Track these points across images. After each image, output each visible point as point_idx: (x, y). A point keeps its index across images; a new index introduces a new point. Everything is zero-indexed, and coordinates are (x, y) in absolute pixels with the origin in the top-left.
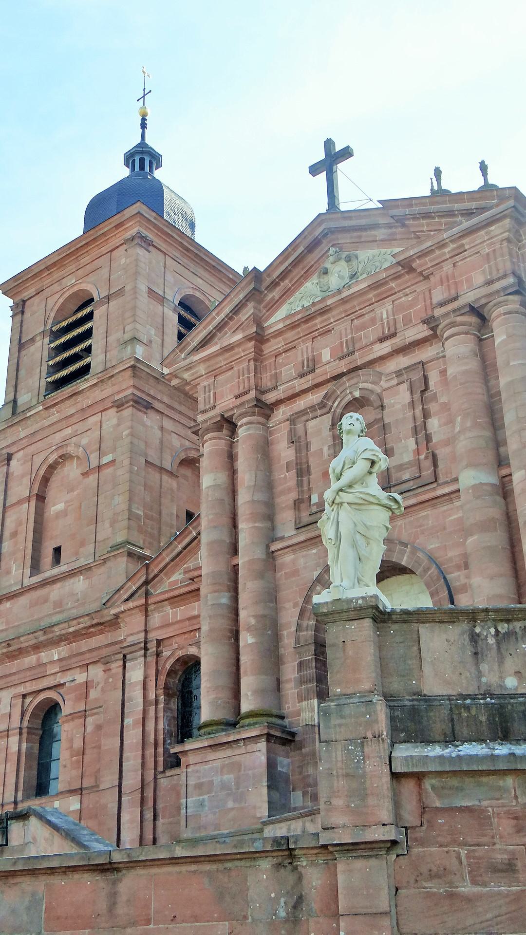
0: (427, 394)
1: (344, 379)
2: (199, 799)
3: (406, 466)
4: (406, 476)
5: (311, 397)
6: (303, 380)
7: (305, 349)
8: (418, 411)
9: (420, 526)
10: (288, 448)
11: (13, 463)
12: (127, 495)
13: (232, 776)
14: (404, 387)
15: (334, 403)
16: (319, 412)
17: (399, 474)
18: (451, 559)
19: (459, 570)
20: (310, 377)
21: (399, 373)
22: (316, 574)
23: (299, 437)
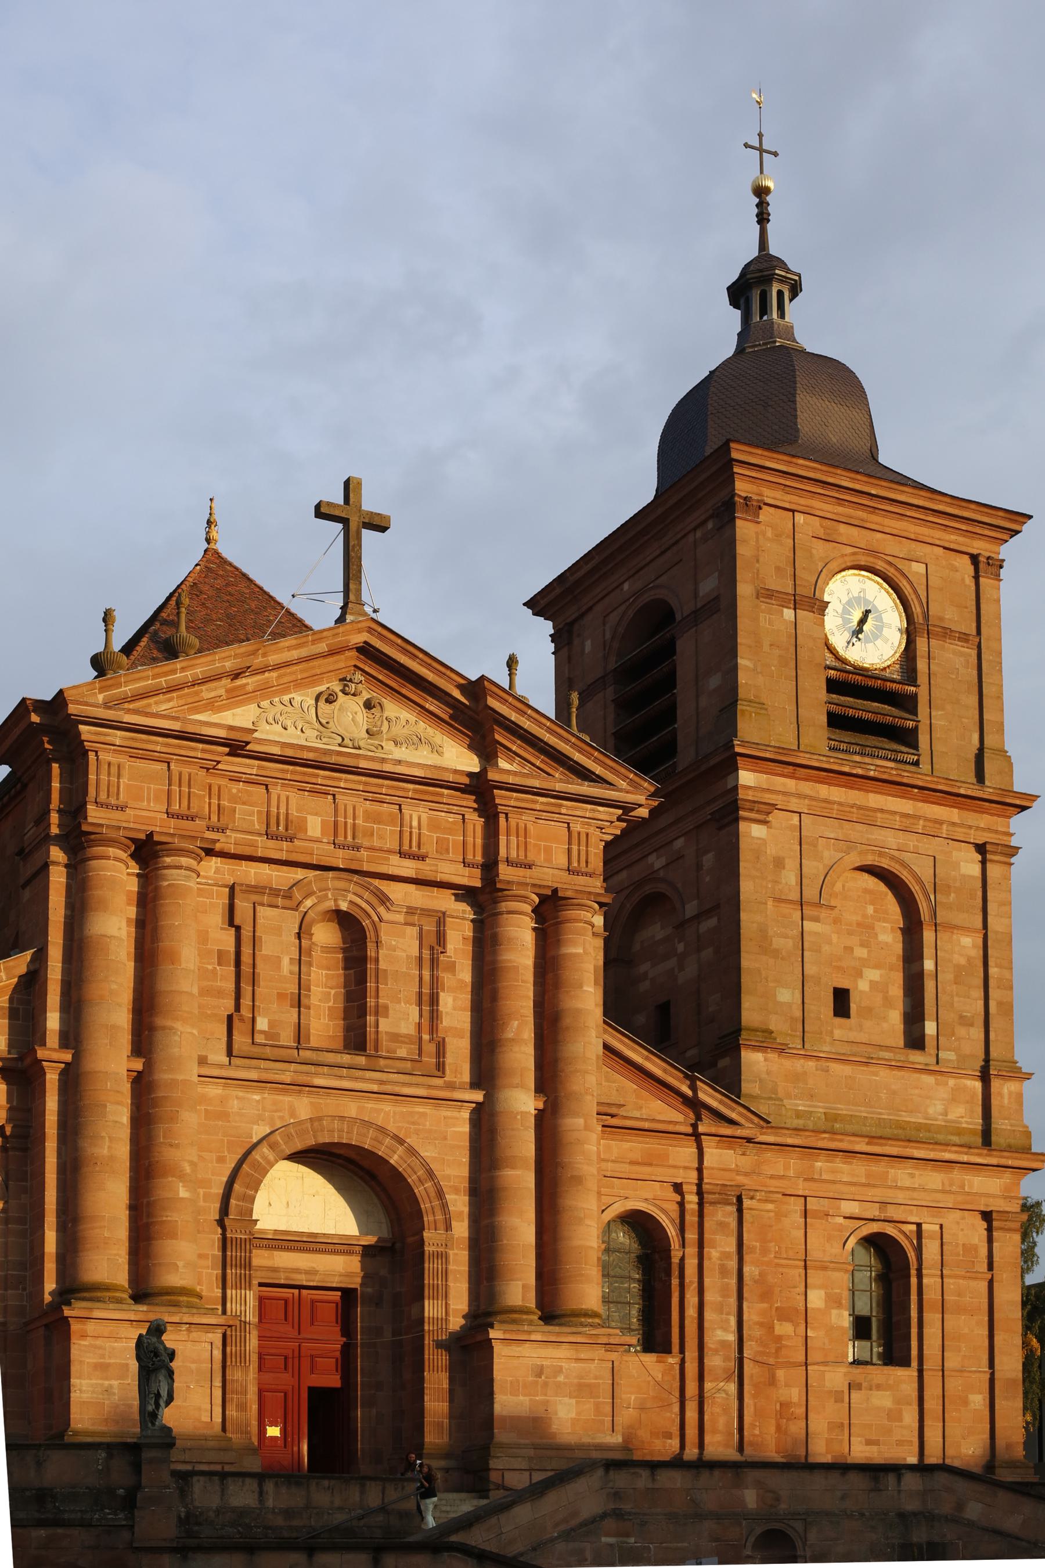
1: (331, 874)
4: (402, 1052)
6: (271, 843)
7: (283, 799)
8: (426, 974)
9: (414, 1123)
14: (413, 931)
16: (280, 901)
17: (393, 1045)
20: (285, 845)
21: (411, 911)
22: (259, 1131)
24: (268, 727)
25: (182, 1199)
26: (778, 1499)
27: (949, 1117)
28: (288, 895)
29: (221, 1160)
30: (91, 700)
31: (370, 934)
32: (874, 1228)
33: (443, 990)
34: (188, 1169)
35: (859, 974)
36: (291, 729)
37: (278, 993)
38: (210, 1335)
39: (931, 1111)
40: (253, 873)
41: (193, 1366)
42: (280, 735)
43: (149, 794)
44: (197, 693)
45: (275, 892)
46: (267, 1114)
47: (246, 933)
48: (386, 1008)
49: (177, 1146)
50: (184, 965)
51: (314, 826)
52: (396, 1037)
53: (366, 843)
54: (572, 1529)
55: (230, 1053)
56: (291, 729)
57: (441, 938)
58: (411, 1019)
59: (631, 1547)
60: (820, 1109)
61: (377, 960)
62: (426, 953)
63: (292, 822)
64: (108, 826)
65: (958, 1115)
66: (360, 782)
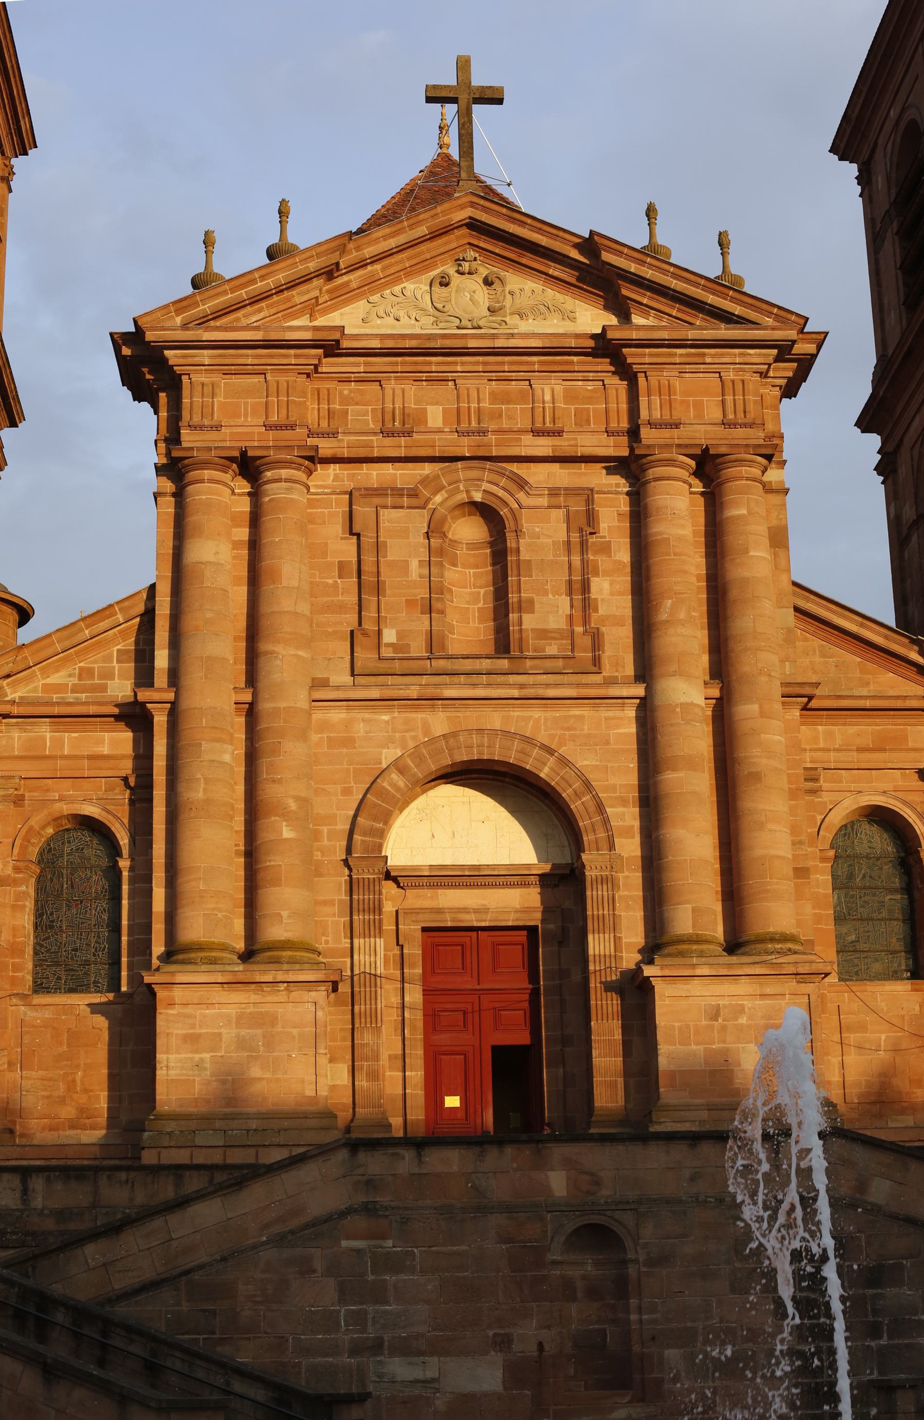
1: (459, 464)
2: (192, 1059)
3: (552, 635)
4: (552, 650)
5: (392, 471)
6: (388, 441)
7: (398, 392)
8: (576, 559)
10: (342, 539)
13: (260, 1031)
14: (560, 514)
16: (405, 501)
18: (613, 788)
19: (624, 806)
21: (554, 492)
22: (389, 755)
24: (379, 321)
25: (286, 839)
26: (597, 1183)
28: (413, 493)
29: (347, 791)
30: (169, 324)
31: (509, 524)
33: (597, 574)
34: (293, 805)
36: (404, 320)
37: (407, 600)
38: (313, 994)
40: (374, 474)
41: (295, 1031)
42: (393, 327)
43: (246, 409)
45: (398, 492)
46: (397, 735)
47: (368, 540)
48: (531, 602)
49: (279, 781)
50: (284, 583)
51: (435, 416)
52: (543, 634)
53: (492, 426)
54: (292, 1232)
55: (353, 674)
56: (404, 320)
57: (591, 517)
58: (561, 612)
59: (388, 1253)
61: (518, 550)
62: (575, 537)
63: (409, 416)
64: (199, 449)
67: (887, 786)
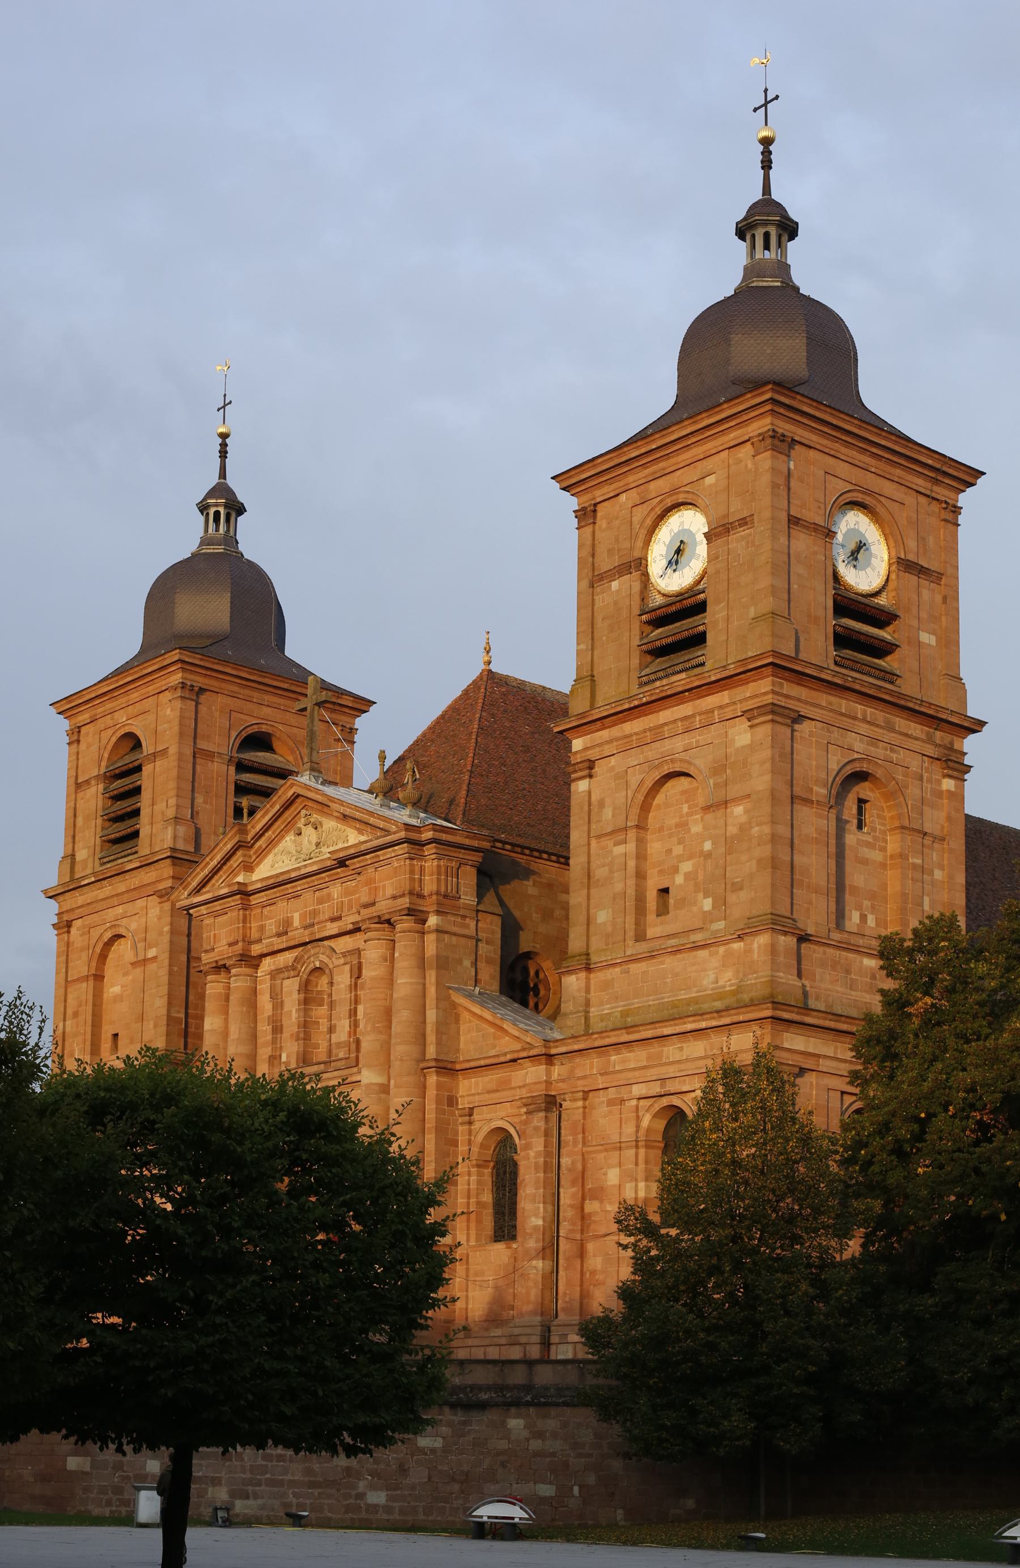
0: (360, 981)
6: (279, 940)
11: (73, 930)
12: (166, 999)
15: (302, 967)
23: (277, 995)
27: (719, 984)
28: (293, 968)
32: (665, 1102)
35: (676, 870)
39: (705, 982)
44: (231, 866)
52: (339, 1045)
60: (620, 1006)
65: (726, 979)
66: (276, 893)
67: (503, 1114)
